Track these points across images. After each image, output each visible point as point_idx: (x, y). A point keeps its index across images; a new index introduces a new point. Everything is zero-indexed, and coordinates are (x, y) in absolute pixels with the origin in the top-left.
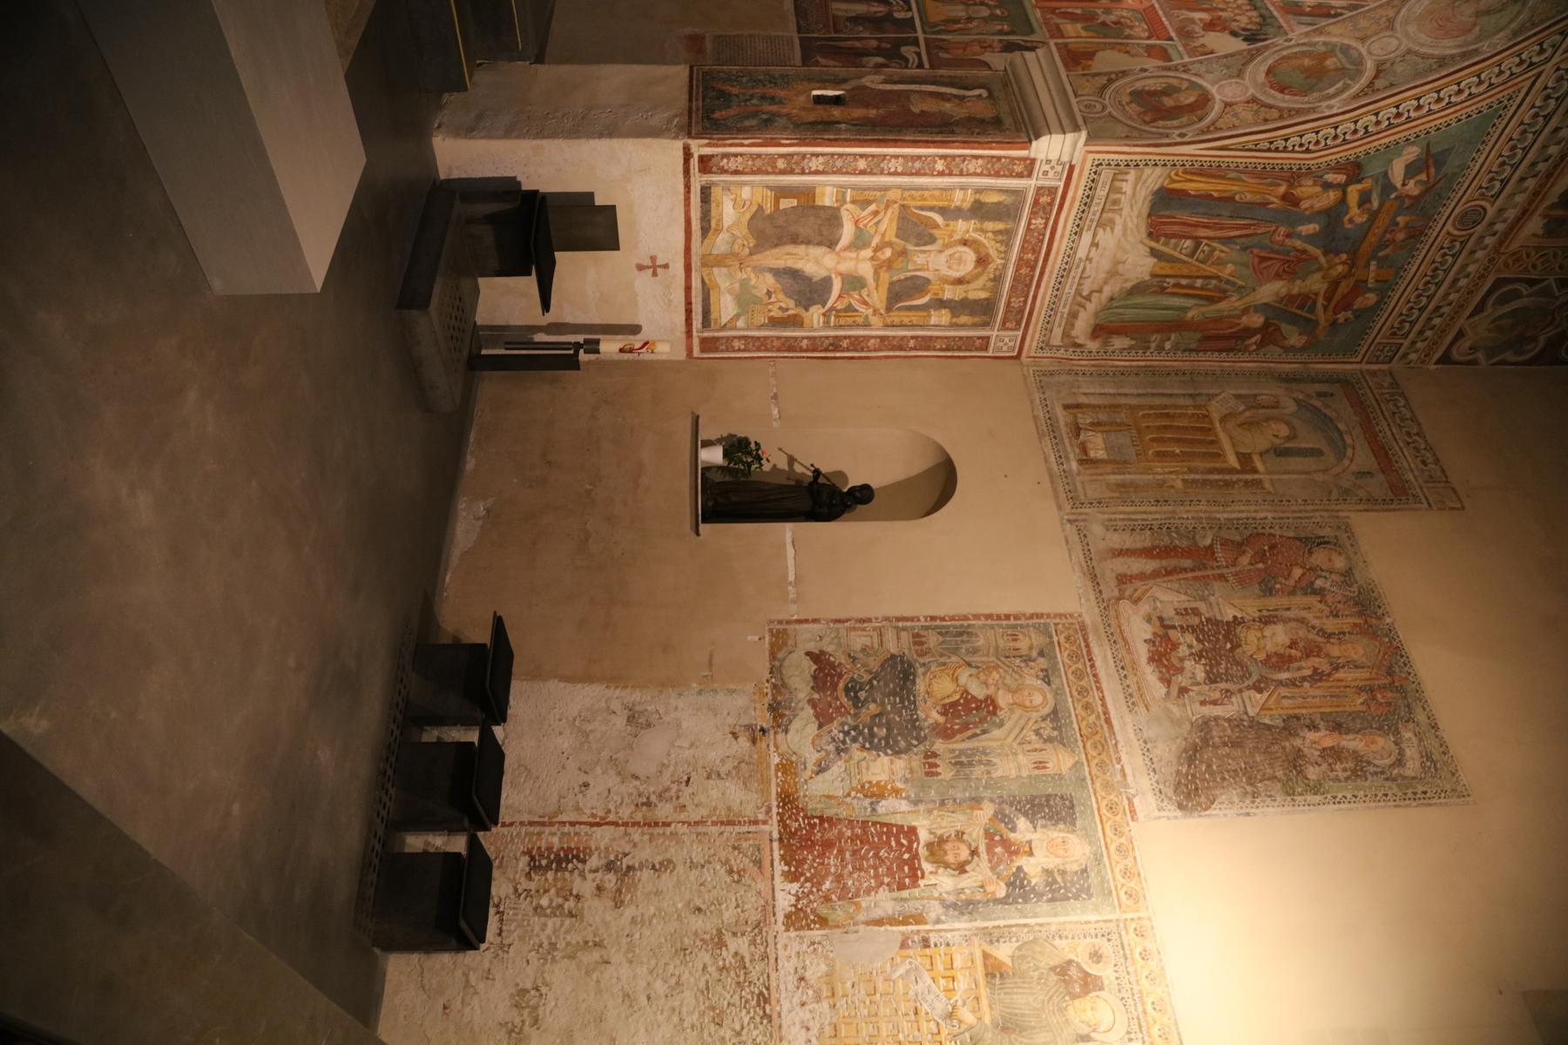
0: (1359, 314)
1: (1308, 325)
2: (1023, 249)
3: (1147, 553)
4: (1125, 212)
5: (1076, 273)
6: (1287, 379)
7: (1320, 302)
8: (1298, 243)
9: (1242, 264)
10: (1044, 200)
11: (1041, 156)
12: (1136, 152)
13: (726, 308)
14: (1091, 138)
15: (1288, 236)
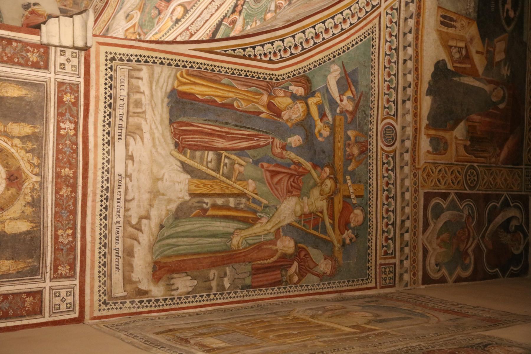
2: (58, 161)
4: (149, 115)
5: (119, 194)
7: (327, 221)
8: (293, 155)
9: (260, 181)
10: (68, 98)
11: (55, 41)
15: (284, 148)
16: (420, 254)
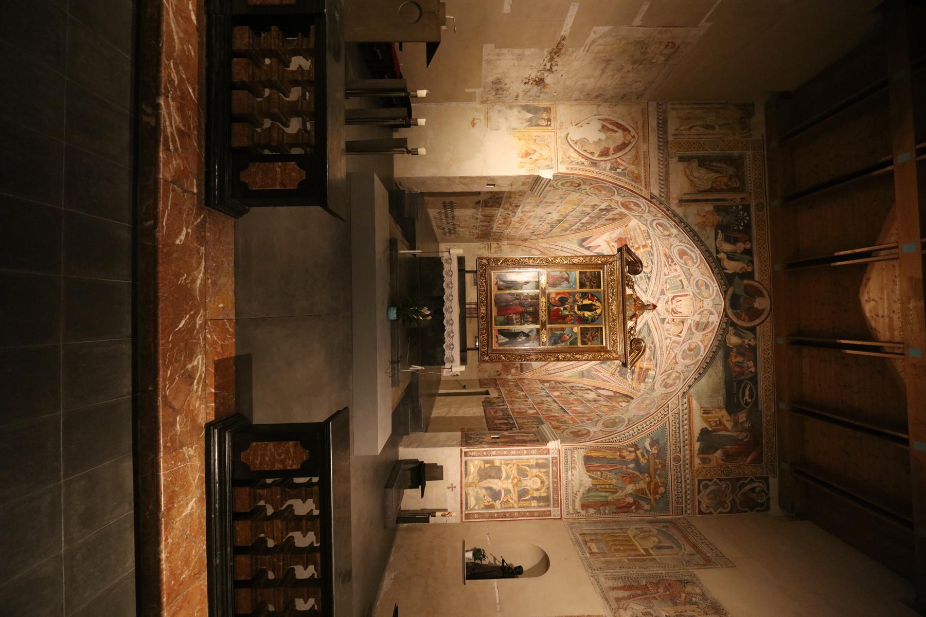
0: (662, 495)
1: (648, 501)
3: (623, 588)
5: (570, 485)
6: (651, 522)
12: (575, 445)
13: (472, 502)
14: (562, 442)
16: (697, 503)
